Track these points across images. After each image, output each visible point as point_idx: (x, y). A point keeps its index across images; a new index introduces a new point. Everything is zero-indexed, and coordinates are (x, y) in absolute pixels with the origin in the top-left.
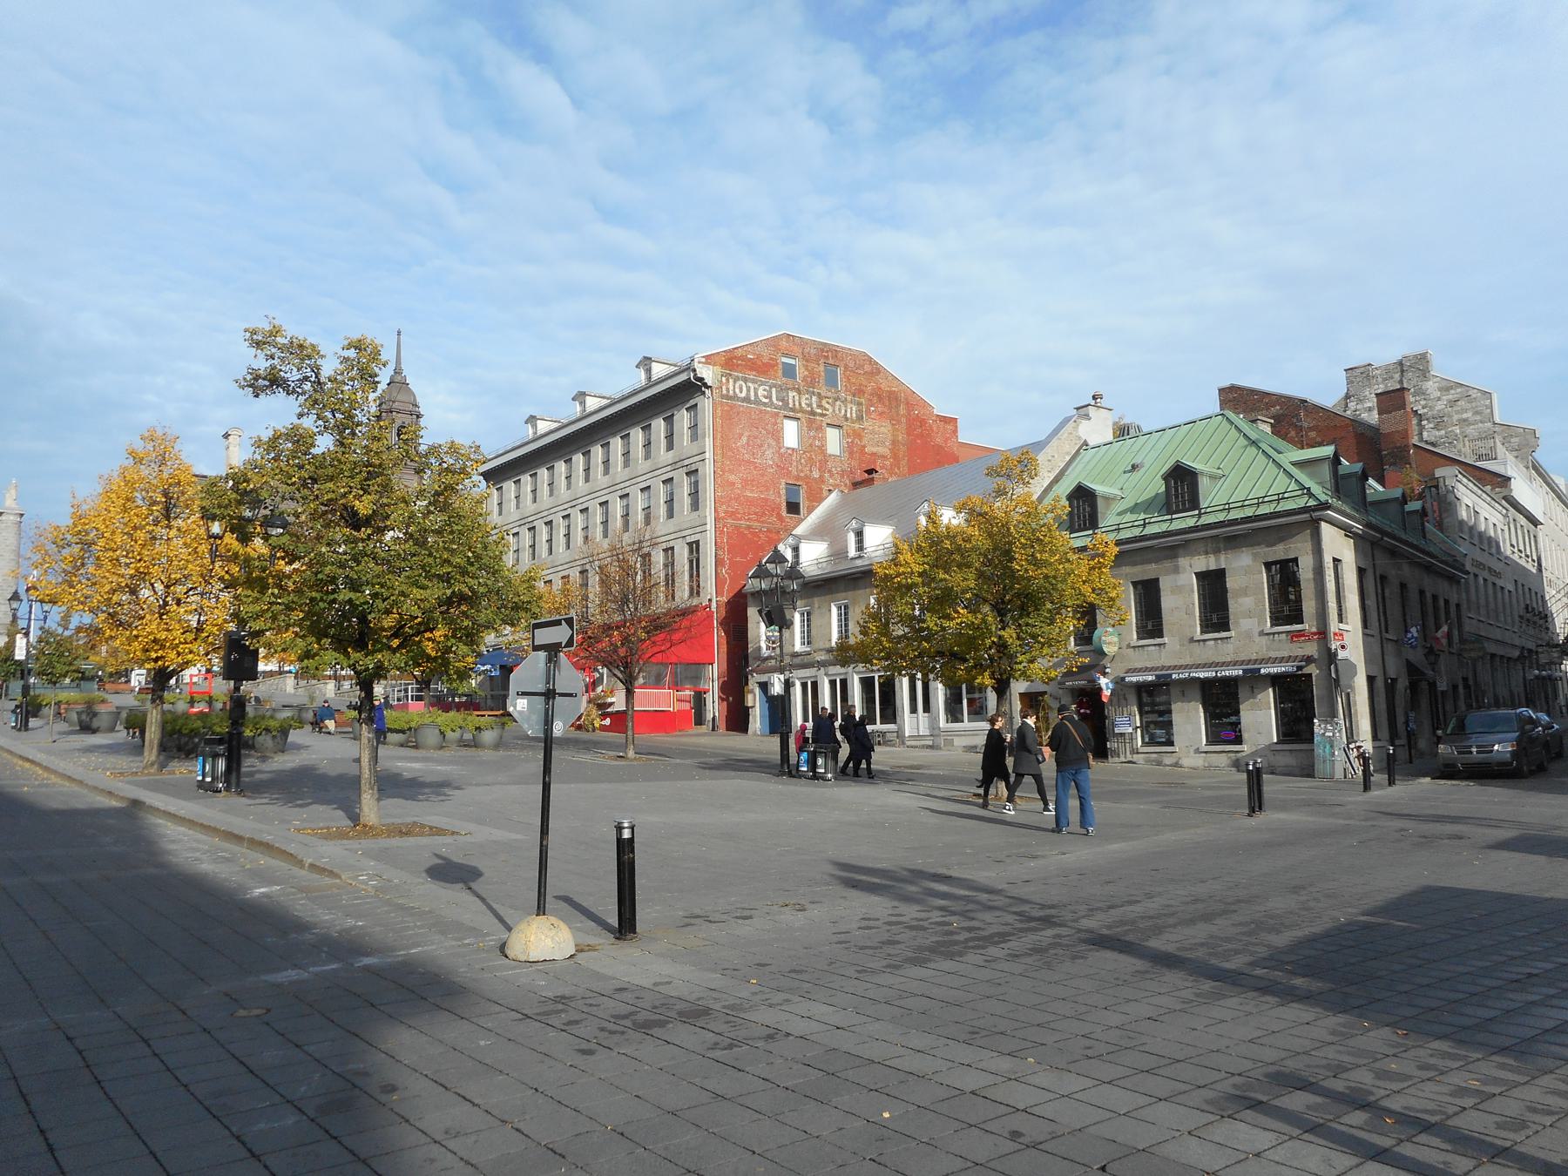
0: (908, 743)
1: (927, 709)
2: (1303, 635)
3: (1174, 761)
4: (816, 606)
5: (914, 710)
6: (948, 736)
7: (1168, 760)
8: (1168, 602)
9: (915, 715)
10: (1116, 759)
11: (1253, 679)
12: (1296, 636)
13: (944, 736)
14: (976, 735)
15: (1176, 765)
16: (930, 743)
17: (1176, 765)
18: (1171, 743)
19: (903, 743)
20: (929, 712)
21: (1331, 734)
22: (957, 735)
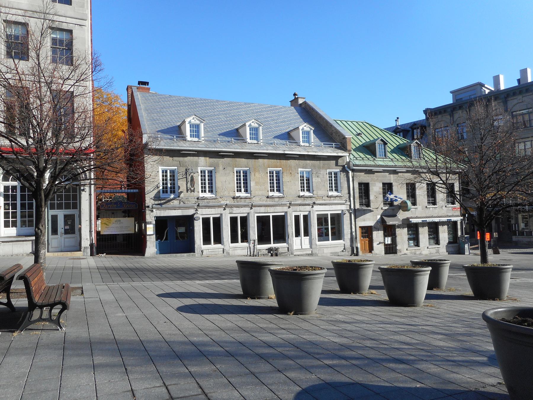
0: (295, 253)
1: (306, 234)
2: (456, 209)
3: (420, 252)
4: (221, 168)
5: (298, 234)
6: (320, 248)
7: (418, 253)
8: (418, 192)
9: (299, 238)
10: (400, 254)
11: (443, 223)
12: (454, 209)
13: (318, 248)
14: (337, 247)
15: (420, 254)
16: (310, 252)
17: (420, 254)
18: (419, 246)
19: (292, 254)
20: (307, 236)
21: (464, 240)
22: (327, 248)
